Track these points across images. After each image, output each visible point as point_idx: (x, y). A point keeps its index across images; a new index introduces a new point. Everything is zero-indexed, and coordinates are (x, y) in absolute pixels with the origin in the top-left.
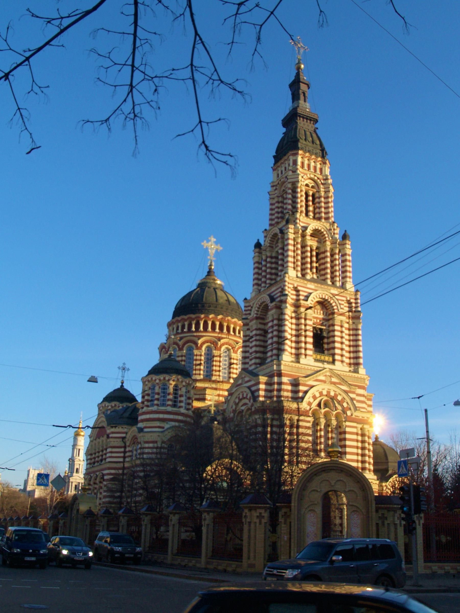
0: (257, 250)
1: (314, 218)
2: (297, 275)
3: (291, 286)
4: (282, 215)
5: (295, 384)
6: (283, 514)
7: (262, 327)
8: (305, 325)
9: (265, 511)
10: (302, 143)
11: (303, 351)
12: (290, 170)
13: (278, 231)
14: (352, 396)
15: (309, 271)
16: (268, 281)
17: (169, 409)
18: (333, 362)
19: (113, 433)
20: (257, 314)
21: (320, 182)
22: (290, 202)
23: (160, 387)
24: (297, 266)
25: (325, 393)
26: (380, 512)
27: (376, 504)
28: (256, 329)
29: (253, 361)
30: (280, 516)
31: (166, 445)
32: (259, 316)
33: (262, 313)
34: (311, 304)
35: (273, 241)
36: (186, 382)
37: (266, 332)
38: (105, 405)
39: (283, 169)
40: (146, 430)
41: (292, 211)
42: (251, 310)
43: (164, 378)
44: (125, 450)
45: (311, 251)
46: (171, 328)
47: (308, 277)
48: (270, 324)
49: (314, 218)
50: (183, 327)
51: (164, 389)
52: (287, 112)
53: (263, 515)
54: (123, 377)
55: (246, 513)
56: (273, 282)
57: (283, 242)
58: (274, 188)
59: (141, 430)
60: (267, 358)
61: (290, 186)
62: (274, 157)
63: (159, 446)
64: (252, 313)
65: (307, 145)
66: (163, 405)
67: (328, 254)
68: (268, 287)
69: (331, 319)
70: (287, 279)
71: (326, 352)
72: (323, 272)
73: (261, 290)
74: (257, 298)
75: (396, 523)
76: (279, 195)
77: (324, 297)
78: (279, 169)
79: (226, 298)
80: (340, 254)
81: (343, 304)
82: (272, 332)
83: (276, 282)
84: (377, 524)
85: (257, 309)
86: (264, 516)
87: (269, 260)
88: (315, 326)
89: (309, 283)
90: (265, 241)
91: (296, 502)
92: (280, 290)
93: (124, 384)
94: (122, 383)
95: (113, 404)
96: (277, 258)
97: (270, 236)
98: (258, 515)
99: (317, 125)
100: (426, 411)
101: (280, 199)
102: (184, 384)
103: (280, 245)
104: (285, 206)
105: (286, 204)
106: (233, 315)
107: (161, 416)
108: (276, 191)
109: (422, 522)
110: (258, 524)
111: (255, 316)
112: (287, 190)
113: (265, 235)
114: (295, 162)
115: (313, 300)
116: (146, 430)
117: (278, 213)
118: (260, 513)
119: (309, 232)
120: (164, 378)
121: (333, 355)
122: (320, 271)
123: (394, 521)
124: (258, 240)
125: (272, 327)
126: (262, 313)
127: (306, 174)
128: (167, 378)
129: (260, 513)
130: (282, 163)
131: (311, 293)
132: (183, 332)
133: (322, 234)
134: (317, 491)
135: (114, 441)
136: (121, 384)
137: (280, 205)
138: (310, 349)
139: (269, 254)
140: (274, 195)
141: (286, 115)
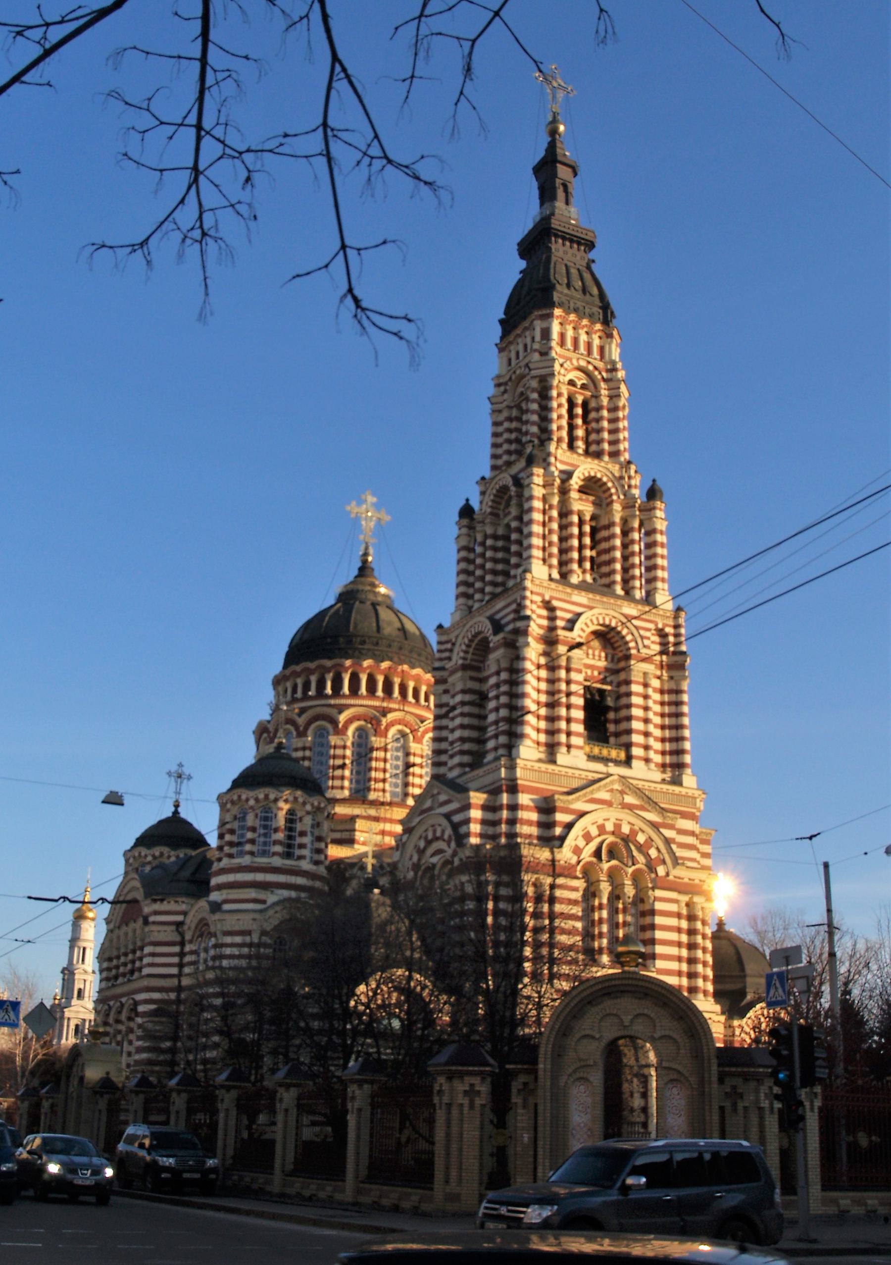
0: (465, 522)
1: (587, 453)
2: (550, 575)
3: (538, 599)
4: (519, 447)
5: (547, 807)
6: (521, 1087)
8: (568, 682)
9: (483, 1079)
10: (561, 293)
11: (563, 738)
12: (536, 350)
13: (509, 481)
14: (669, 833)
15: (575, 566)
16: (488, 589)
17: (277, 862)
18: (628, 761)
19: (156, 913)
20: (464, 659)
21: (599, 377)
22: (535, 418)
23: (256, 816)
24: (551, 555)
25: (610, 827)
26: (729, 1082)
27: (719, 1065)
28: (463, 692)
29: (457, 760)
30: (514, 1091)
31: (270, 939)
32: (468, 662)
33: (475, 657)
35: (500, 503)
36: (312, 805)
37: (483, 697)
38: (140, 853)
39: (521, 348)
40: (226, 907)
41: (539, 438)
42: (451, 650)
43: (267, 797)
44: (182, 949)
45: (581, 523)
46: (280, 689)
47: (574, 579)
48: (493, 681)
49: (587, 453)
50: (307, 686)
51: (266, 819)
52: (530, 225)
53: (477, 1088)
54: (178, 793)
55: (441, 1085)
56: (499, 590)
57: (520, 505)
58: (502, 389)
59: (216, 907)
60: (486, 752)
61: (534, 384)
62: (502, 322)
63: (256, 940)
64: (455, 657)
65: (572, 297)
66: (264, 853)
67: (618, 530)
68: (488, 602)
69: (623, 669)
70: (528, 584)
71: (612, 740)
72: (605, 569)
73: (472, 607)
74: (464, 626)
75: (762, 1105)
76: (513, 404)
77: (607, 622)
78: (512, 347)
79: (398, 625)
80: (643, 531)
81: (648, 638)
82: (497, 697)
83: (506, 590)
84: (722, 1109)
85: (464, 647)
86: (479, 1092)
87: (489, 542)
88: (588, 684)
89: (576, 592)
90: (481, 502)
91: (549, 1062)
92: (514, 606)
93: (180, 809)
94: (177, 806)
95: (157, 851)
96: (507, 538)
98: (467, 1088)
99: (592, 255)
100: (826, 866)
101: (515, 413)
102: (308, 807)
103: (514, 511)
104: (524, 429)
105: (527, 422)
106: (413, 660)
107: (260, 877)
108: (506, 396)
109: (818, 1103)
110: (466, 1109)
111: (460, 662)
112: (528, 393)
113: (483, 489)
114: (546, 334)
115: (585, 628)
116: (226, 907)
117: (509, 441)
118: (472, 1085)
119: (576, 482)
120: (267, 797)
121: (628, 746)
122: (600, 565)
123: (757, 1100)
124: (467, 500)
125: (497, 686)
126: (475, 657)
127: (570, 359)
128: (272, 797)
129: (472, 1085)
130: (519, 336)
131: (579, 615)
132: (306, 697)
133: (604, 488)
134: (593, 1037)
135: (159, 931)
136: (173, 809)
137: (514, 425)
138: (578, 735)
139: (489, 530)
140: (501, 403)
141: (526, 232)
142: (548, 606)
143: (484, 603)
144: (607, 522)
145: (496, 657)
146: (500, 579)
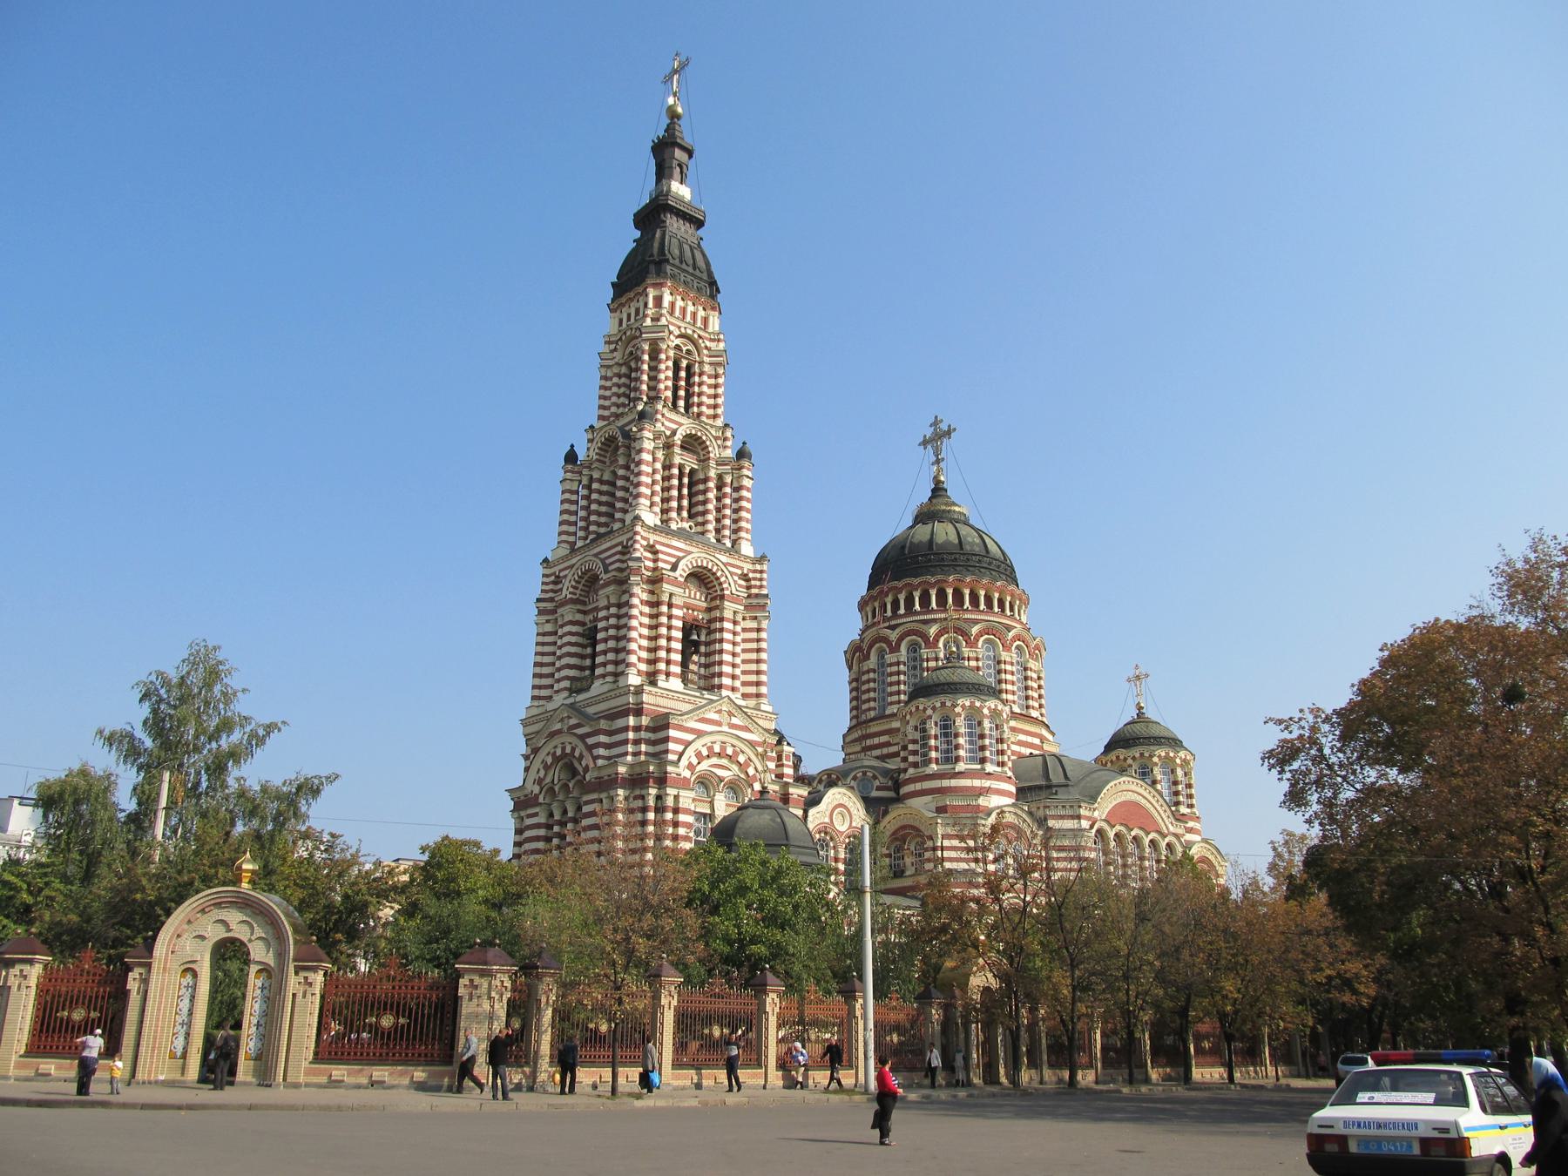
7: (579, 617)
11: (662, 666)
15: (674, 515)
21: (703, 345)
34: (681, 575)
48: (602, 614)
56: (602, 530)
58: (612, 347)
62: (613, 284)
67: (711, 484)
69: (717, 607)
72: (700, 519)
76: (621, 362)
77: (705, 565)
83: (611, 532)
90: (588, 449)
92: (619, 548)
96: (613, 484)
97: (600, 439)
99: (701, 232)
101: (624, 370)
103: (621, 461)
112: (639, 353)
113: (591, 437)
114: (658, 301)
124: (572, 446)
125: (607, 618)
130: (631, 300)
131: (679, 559)
133: (703, 446)
137: (623, 380)
141: (643, 204)
142: (651, 549)
143: (588, 541)
144: (701, 476)
145: (606, 595)
146: (603, 520)
